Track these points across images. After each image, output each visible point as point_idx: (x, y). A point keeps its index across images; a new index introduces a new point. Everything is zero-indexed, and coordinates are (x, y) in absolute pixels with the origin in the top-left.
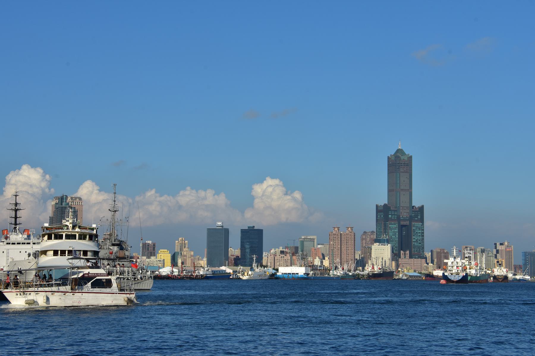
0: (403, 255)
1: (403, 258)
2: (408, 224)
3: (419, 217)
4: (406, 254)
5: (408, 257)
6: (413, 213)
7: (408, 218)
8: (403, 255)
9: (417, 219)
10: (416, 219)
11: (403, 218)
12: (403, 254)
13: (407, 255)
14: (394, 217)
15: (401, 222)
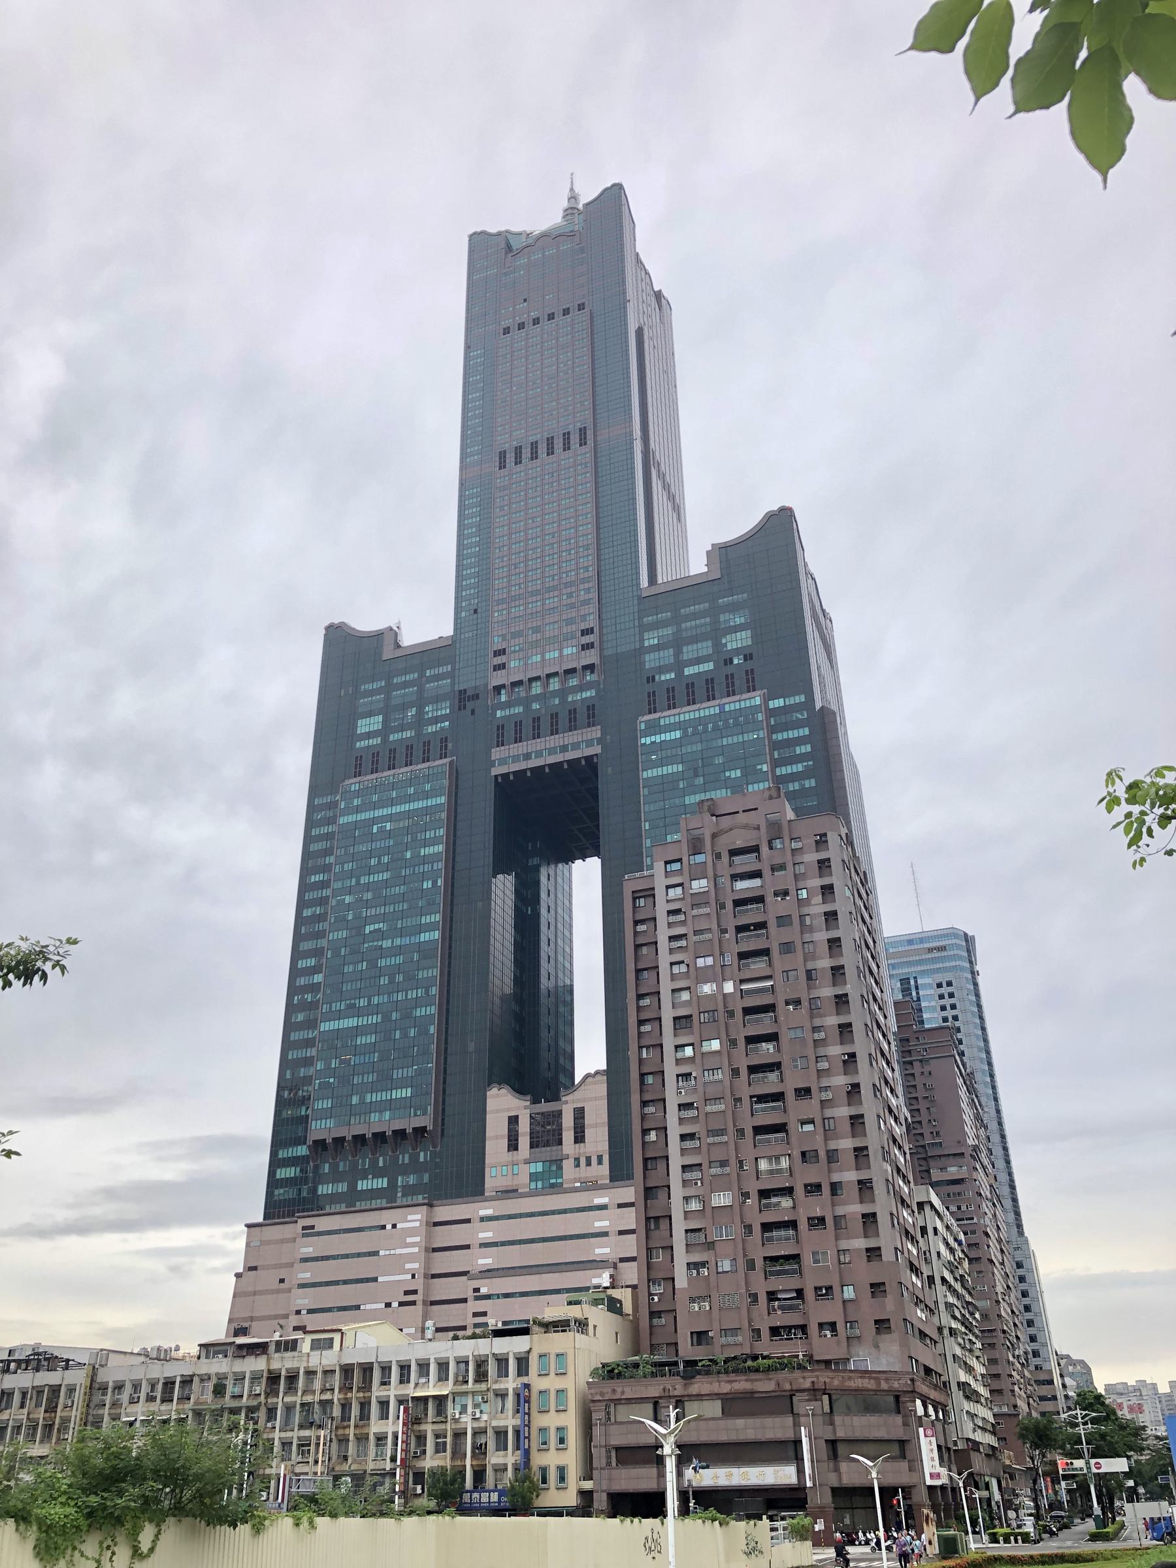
0: (513, 1146)
1: (510, 1193)
2: (596, 750)
3: (739, 641)
4: (568, 1121)
5: (605, 1169)
6: (643, 628)
7: (581, 688)
8: (524, 1142)
9: (710, 666)
10: (688, 671)
11: (527, 702)
12: (524, 1127)
13: (579, 1138)
14: (420, 721)
15: (497, 753)
